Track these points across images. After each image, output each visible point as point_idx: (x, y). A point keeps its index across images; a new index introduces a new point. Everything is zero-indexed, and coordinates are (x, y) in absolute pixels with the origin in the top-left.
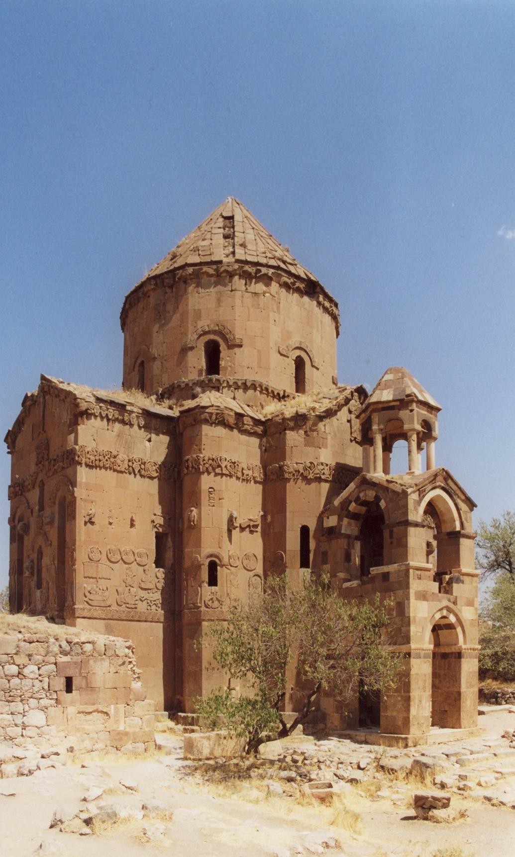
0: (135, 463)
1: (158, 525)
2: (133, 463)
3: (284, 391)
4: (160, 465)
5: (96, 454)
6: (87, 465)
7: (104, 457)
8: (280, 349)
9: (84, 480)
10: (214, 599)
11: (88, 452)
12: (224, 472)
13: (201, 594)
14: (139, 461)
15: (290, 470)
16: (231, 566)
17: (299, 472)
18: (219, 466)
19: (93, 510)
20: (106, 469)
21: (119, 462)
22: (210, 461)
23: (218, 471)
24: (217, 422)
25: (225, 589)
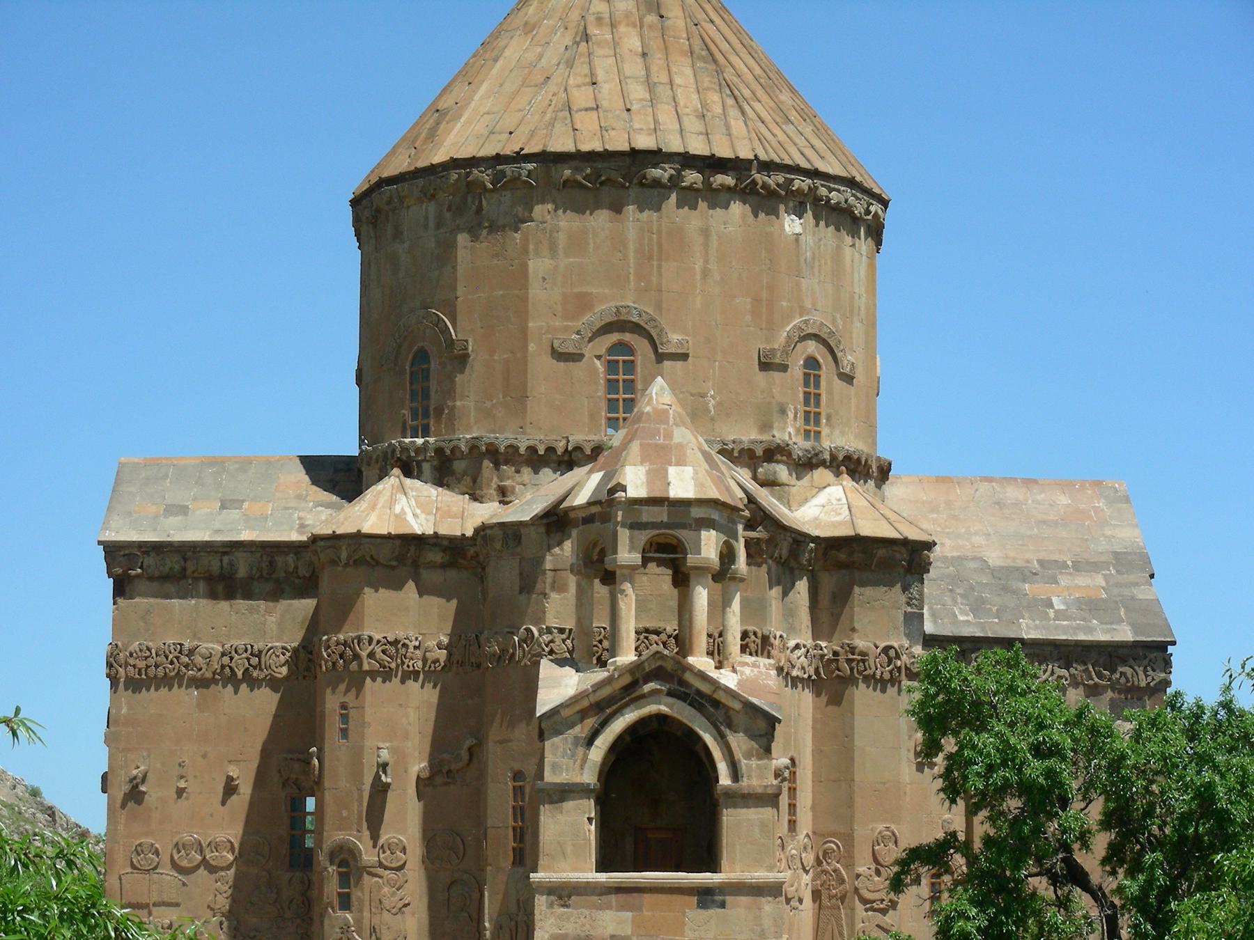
0: (236, 657)
2: (231, 658)
4: (295, 651)
5: (148, 653)
7: (167, 657)
8: (556, 344)
11: (131, 655)
12: (366, 667)
14: (246, 651)
16: (386, 868)
18: (357, 657)
19: (142, 768)
21: (198, 660)
24: (351, 562)
25: (366, 914)
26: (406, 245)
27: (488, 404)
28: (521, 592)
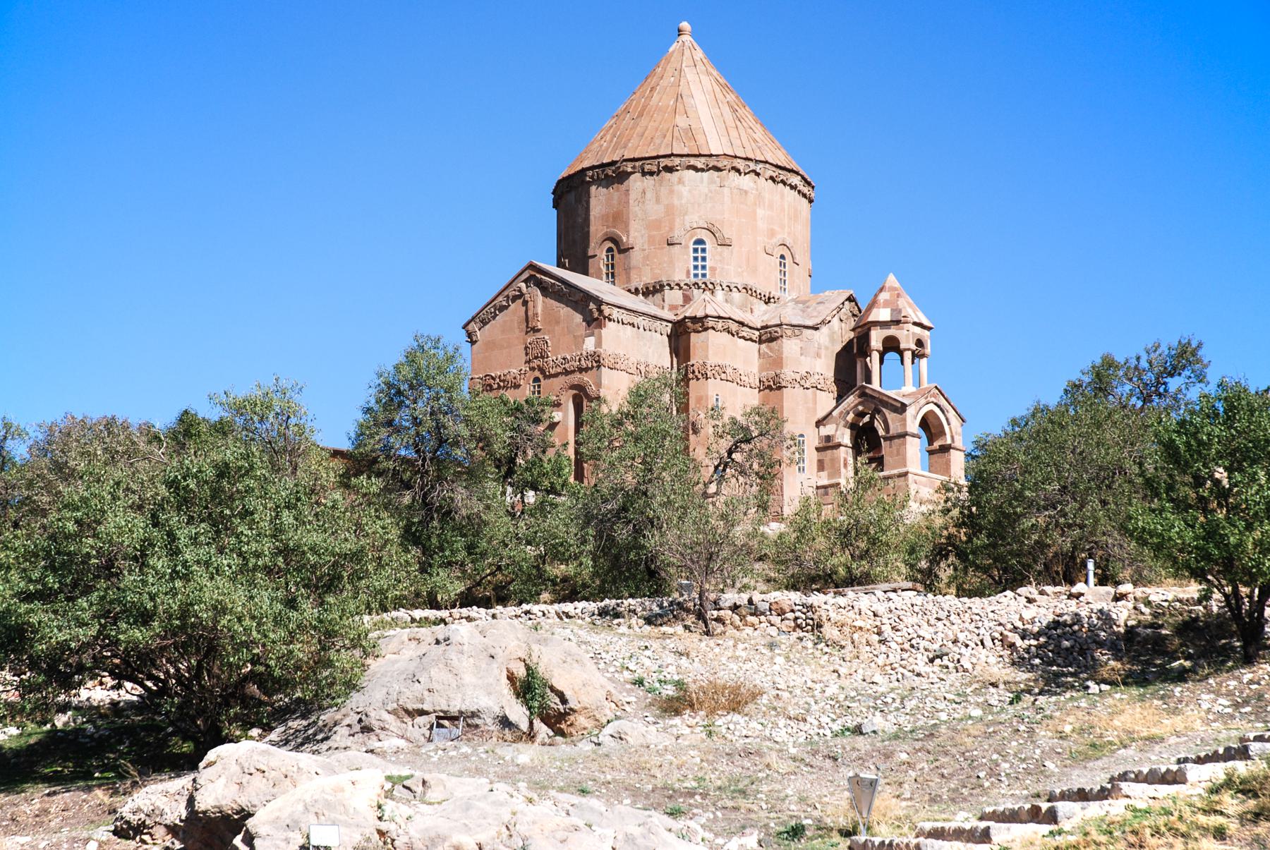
22: (717, 368)
23: (723, 376)
26: (687, 188)
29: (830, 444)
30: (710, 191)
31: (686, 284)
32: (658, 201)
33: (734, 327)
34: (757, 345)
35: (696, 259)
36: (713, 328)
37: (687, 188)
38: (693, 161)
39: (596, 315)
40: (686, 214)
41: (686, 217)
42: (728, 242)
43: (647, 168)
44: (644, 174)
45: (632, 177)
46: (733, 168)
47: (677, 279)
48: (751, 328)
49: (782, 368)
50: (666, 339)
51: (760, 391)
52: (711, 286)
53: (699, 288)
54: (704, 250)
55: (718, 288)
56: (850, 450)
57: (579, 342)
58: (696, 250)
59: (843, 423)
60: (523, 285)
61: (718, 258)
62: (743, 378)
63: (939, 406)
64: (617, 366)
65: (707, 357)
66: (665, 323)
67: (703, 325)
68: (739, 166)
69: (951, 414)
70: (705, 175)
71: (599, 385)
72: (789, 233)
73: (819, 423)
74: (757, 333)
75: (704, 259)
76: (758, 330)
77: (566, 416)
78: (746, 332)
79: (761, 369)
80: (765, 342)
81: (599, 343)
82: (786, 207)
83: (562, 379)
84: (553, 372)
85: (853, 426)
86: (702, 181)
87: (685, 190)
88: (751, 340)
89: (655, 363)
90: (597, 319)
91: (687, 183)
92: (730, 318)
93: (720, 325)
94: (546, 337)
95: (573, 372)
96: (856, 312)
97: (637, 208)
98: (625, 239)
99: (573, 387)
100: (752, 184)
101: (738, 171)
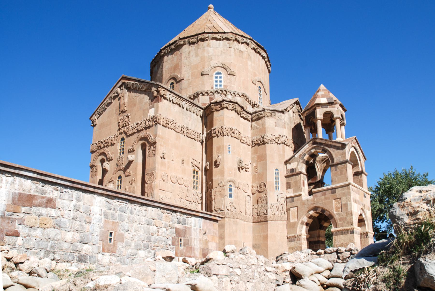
1: (194, 165)
3: (255, 102)
6: (163, 125)
9: (161, 134)
10: (232, 206)
13: (224, 203)
15: (268, 139)
17: (273, 140)
20: (171, 129)
22: (229, 130)
23: (233, 135)
26: (212, 48)
27: (239, 88)
28: (276, 126)
29: (294, 173)
30: (224, 50)
31: (211, 92)
32: (197, 56)
33: (239, 109)
34: (250, 123)
35: (216, 81)
36: (227, 108)
37: (212, 48)
38: (215, 35)
39: (156, 94)
40: (211, 60)
41: (211, 62)
42: (233, 73)
43: (191, 41)
44: (190, 44)
45: (184, 47)
46: (236, 40)
47: (206, 90)
48: (247, 112)
49: (265, 133)
50: (200, 119)
51: (252, 147)
52: (225, 92)
53: (218, 93)
54: (221, 77)
55: (229, 93)
56: (306, 176)
57: (146, 112)
58: (216, 77)
59: (301, 161)
60: (119, 89)
61: (228, 81)
62: (243, 139)
63: (356, 149)
64: (169, 126)
65: (223, 124)
66: (199, 109)
67: (221, 106)
68: (238, 39)
69: (361, 154)
70: (221, 42)
71: (156, 135)
72: (262, 78)
73: (286, 162)
74: (250, 116)
75: (221, 81)
76: (251, 114)
77: (136, 157)
78: (244, 114)
79: (253, 135)
80: (255, 121)
81: (156, 111)
82: (261, 65)
83: (136, 135)
84: (131, 132)
85: (307, 163)
86: (220, 45)
87: (210, 50)
88: (247, 119)
89: (193, 129)
90: (156, 97)
91: (212, 46)
92: (236, 103)
93: (231, 106)
94: (129, 114)
95: (142, 130)
96: (300, 110)
97: (186, 61)
98: (179, 76)
99: (141, 139)
100: (245, 49)
101: (238, 41)
